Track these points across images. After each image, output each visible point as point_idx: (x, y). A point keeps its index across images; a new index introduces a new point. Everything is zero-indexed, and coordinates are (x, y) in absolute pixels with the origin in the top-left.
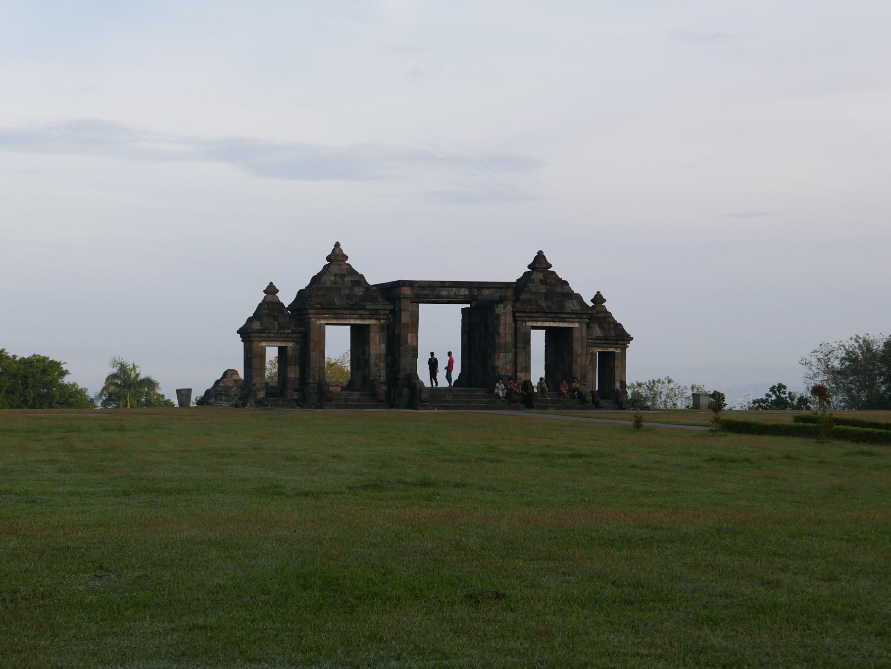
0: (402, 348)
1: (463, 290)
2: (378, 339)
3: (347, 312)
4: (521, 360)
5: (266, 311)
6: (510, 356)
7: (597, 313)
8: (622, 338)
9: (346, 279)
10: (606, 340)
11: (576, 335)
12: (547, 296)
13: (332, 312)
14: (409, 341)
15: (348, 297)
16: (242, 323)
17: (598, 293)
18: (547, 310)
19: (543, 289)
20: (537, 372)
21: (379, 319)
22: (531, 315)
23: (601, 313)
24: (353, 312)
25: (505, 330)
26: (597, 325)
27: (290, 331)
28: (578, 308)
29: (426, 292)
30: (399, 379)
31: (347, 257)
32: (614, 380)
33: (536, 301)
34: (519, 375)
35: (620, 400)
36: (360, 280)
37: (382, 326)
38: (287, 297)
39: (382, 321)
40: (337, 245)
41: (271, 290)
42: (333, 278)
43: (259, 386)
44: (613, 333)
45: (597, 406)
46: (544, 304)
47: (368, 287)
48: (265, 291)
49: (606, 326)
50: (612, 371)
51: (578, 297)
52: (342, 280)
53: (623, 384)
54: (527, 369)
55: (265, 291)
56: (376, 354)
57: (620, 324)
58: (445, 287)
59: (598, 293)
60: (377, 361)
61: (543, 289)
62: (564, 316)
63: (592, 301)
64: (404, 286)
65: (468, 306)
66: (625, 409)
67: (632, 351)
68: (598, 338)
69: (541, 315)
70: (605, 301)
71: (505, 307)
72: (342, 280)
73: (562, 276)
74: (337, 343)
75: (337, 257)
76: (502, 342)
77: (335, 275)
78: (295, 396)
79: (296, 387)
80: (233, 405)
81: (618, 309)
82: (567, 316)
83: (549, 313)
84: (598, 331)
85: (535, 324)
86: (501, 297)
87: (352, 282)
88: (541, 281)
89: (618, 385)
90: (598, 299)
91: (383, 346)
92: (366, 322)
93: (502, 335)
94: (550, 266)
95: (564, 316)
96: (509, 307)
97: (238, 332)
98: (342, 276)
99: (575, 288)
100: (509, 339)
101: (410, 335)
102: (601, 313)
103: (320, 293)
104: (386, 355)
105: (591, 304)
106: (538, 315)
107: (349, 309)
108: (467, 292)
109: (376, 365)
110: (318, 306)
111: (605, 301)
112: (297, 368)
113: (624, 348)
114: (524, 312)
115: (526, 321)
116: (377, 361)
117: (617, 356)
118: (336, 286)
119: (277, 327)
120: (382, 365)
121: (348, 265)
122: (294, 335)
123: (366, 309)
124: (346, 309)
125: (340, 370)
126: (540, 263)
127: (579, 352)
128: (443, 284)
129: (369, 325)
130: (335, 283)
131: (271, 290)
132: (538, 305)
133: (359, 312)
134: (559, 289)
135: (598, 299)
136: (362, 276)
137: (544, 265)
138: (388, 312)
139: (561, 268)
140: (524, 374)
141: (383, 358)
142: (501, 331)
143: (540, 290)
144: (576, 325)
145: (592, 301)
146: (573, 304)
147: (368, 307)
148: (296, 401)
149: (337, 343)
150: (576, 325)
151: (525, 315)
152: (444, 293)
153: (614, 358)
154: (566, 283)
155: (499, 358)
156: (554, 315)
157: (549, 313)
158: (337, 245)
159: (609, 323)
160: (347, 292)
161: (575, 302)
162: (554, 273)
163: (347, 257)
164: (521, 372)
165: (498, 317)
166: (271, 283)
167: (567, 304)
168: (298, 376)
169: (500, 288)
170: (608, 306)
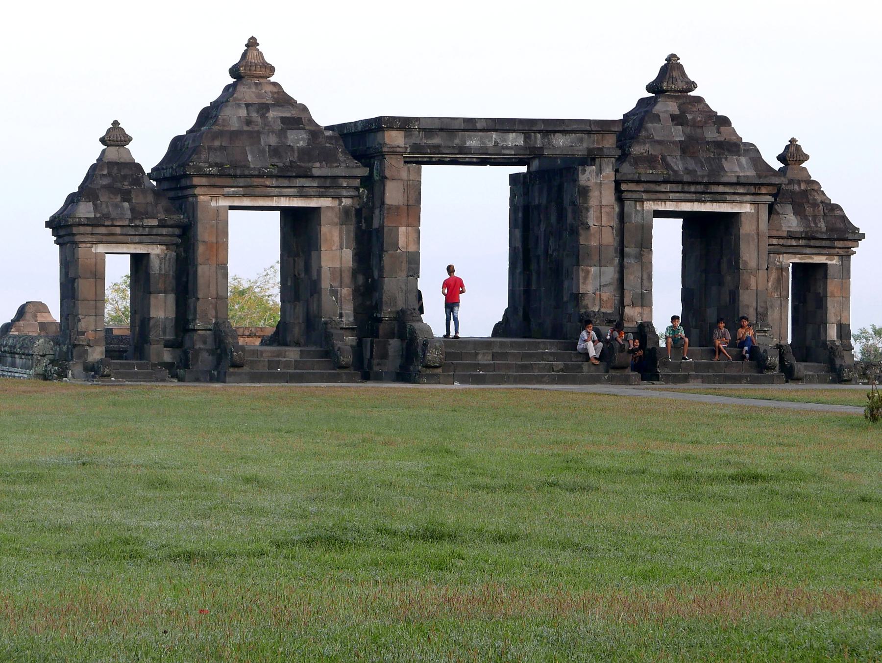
0: (386, 258)
1: (512, 136)
2: (336, 239)
3: (274, 182)
4: (632, 280)
5: (105, 182)
6: (610, 273)
7: (788, 184)
8: (842, 235)
9: (272, 114)
10: (809, 239)
11: (746, 228)
12: (686, 148)
13: (242, 182)
14: (401, 243)
15: (275, 152)
16: (56, 204)
17: (793, 141)
18: (687, 178)
19: (678, 134)
20: (666, 305)
21: (338, 197)
22: (653, 187)
23: (799, 183)
24: (285, 182)
25: (599, 219)
26: (789, 208)
27: (155, 222)
28: (749, 173)
29: (436, 141)
30: (380, 320)
31: (272, 70)
32: (824, 322)
33: (664, 159)
34: (628, 311)
35: (838, 362)
36: (297, 117)
37: (346, 211)
38: (148, 153)
39: (346, 202)
40: (252, 43)
41: (116, 137)
42: (243, 112)
43: (90, 335)
44: (822, 225)
45: (790, 375)
46: (678, 165)
47: (316, 131)
48: (103, 140)
49: (809, 210)
50: (821, 303)
51: (752, 152)
52: (263, 116)
53: (844, 330)
54: (645, 299)
55: (103, 140)
56: (333, 270)
57: (837, 207)
58: (476, 130)
59: (793, 141)
60: (336, 284)
61: (678, 134)
62: (721, 189)
63: (781, 158)
64: (391, 128)
65: (523, 169)
66: (848, 381)
67: (862, 261)
68: (791, 236)
69: (675, 187)
70: (806, 157)
71: (600, 171)
72: (263, 116)
73: (719, 107)
74: (251, 247)
75: (250, 69)
76: (594, 243)
77: (248, 105)
78: (167, 356)
79: (170, 336)
80: (37, 375)
81: (832, 175)
82: (727, 190)
83: (690, 183)
84: (791, 222)
85: (661, 207)
86: (590, 150)
87: (284, 120)
88: (673, 117)
89: (832, 333)
90: (793, 155)
91: (348, 256)
92: (313, 203)
93: (593, 229)
94: (692, 86)
95: (721, 189)
96: (608, 172)
97: (48, 224)
98: (263, 108)
99: (745, 130)
100: (609, 238)
101: (402, 230)
102: (799, 183)
103: (217, 143)
104: (355, 273)
105: (777, 165)
106: (668, 187)
107: (277, 177)
108: (520, 141)
109: (334, 292)
110: (213, 170)
111: (806, 157)
112: (171, 298)
113: (846, 256)
114: (638, 182)
115: (642, 201)
116: (336, 284)
117: (830, 271)
118: (250, 134)
119: (129, 214)
120: (346, 292)
121: (275, 84)
122: (164, 231)
123: (313, 177)
124: (270, 176)
125: (260, 302)
126: (671, 81)
127: (753, 264)
128: (470, 125)
129: (317, 210)
130: (249, 122)
131: (116, 137)
132: (668, 166)
133: (299, 182)
134: (711, 134)
135: (793, 155)
136: (304, 109)
137: (681, 85)
138: (357, 182)
139: (714, 91)
140: (638, 309)
141: (347, 279)
142: (591, 223)
143: (671, 135)
144: (747, 208)
145: (781, 158)
146: (740, 165)
147: (316, 172)
148: (169, 366)
149: (251, 247)
150: (747, 208)
151: (640, 188)
152: (473, 142)
153: (825, 277)
154: (725, 121)
156: (700, 188)
157: (690, 183)
158: (252, 43)
159: (815, 205)
160: (273, 140)
161: (743, 160)
162: (700, 100)
163: (272, 70)
164: (633, 305)
165: (584, 192)
166: (116, 123)
167: (726, 165)
168: (172, 315)
169: (589, 132)
170: (814, 168)
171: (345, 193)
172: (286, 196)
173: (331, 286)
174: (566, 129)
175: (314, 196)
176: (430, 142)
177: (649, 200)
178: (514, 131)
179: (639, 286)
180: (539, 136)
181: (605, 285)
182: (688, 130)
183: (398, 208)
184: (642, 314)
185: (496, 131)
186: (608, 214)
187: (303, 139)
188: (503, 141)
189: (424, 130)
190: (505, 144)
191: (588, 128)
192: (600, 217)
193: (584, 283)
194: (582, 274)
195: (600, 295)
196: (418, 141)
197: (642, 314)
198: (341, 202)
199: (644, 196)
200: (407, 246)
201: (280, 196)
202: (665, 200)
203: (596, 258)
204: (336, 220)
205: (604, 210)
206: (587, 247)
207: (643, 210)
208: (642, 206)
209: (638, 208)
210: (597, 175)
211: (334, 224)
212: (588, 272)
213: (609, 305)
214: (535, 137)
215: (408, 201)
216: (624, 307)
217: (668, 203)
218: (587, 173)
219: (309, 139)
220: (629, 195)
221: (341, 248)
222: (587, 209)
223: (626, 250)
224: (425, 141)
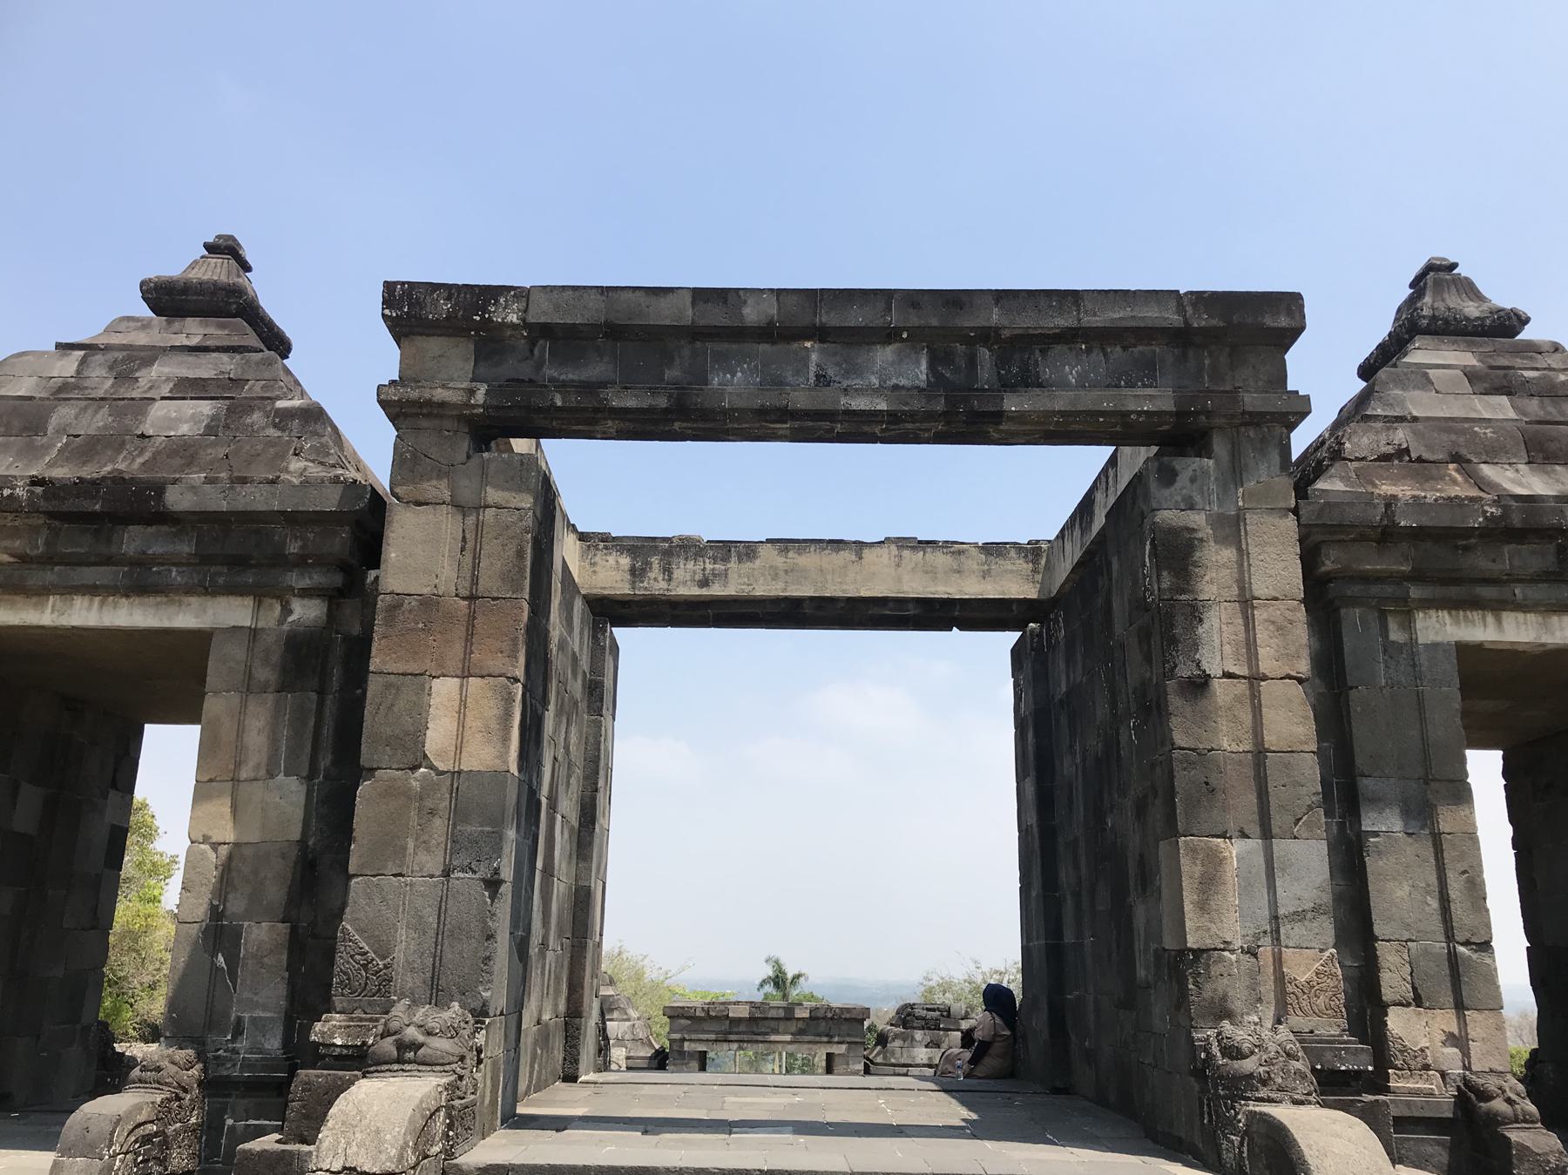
1: (884, 355)
2: (256, 738)
6: (1308, 862)
14: (438, 736)
21: (259, 594)
24: (82, 544)
39: (306, 612)
72: (124, 376)
76: (1229, 739)
92: (186, 616)
100: (1290, 722)
101: (444, 690)
129: (200, 640)
133: (132, 540)
142: (1213, 667)
155: (1210, 883)
171: (296, 580)
172: (91, 590)
173: (216, 913)
174: (1088, 321)
175: (189, 591)
176: (571, 375)
177: (1429, 604)
178: (889, 335)
179: (1436, 925)
180: (984, 354)
181: (1299, 916)
182: (1533, 406)
183: (429, 603)
184: (1459, 1040)
185: (822, 334)
186: (1280, 629)
187: (194, 418)
188: (847, 374)
189: (544, 331)
190: (857, 382)
191: (1173, 318)
192: (1251, 646)
193: (1203, 906)
194: (1190, 870)
195: (1278, 961)
196: (525, 371)
197: (1459, 1040)
198: (287, 610)
199: (1415, 592)
200: (459, 748)
201: (70, 590)
202: (1498, 607)
203: (1247, 801)
204: (264, 674)
205: (1260, 615)
206: (1202, 756)
207: (1413, 642)
208: (1408, 625)
209: (1396, 635)
210: (1224, 487)
211: (249, 687)
212: (1215, 861)
213: (1321, 1001)
214: (972, 361)
215: (475, 581)
216: (1382, 1008)
217: (1509, 618)
218: (1183, 479)
219: (214, 418)
220: (1355, 590)
221: (271, 775)
222: (1195, 613)
223: (1367, 785)
224: (550, 372)
